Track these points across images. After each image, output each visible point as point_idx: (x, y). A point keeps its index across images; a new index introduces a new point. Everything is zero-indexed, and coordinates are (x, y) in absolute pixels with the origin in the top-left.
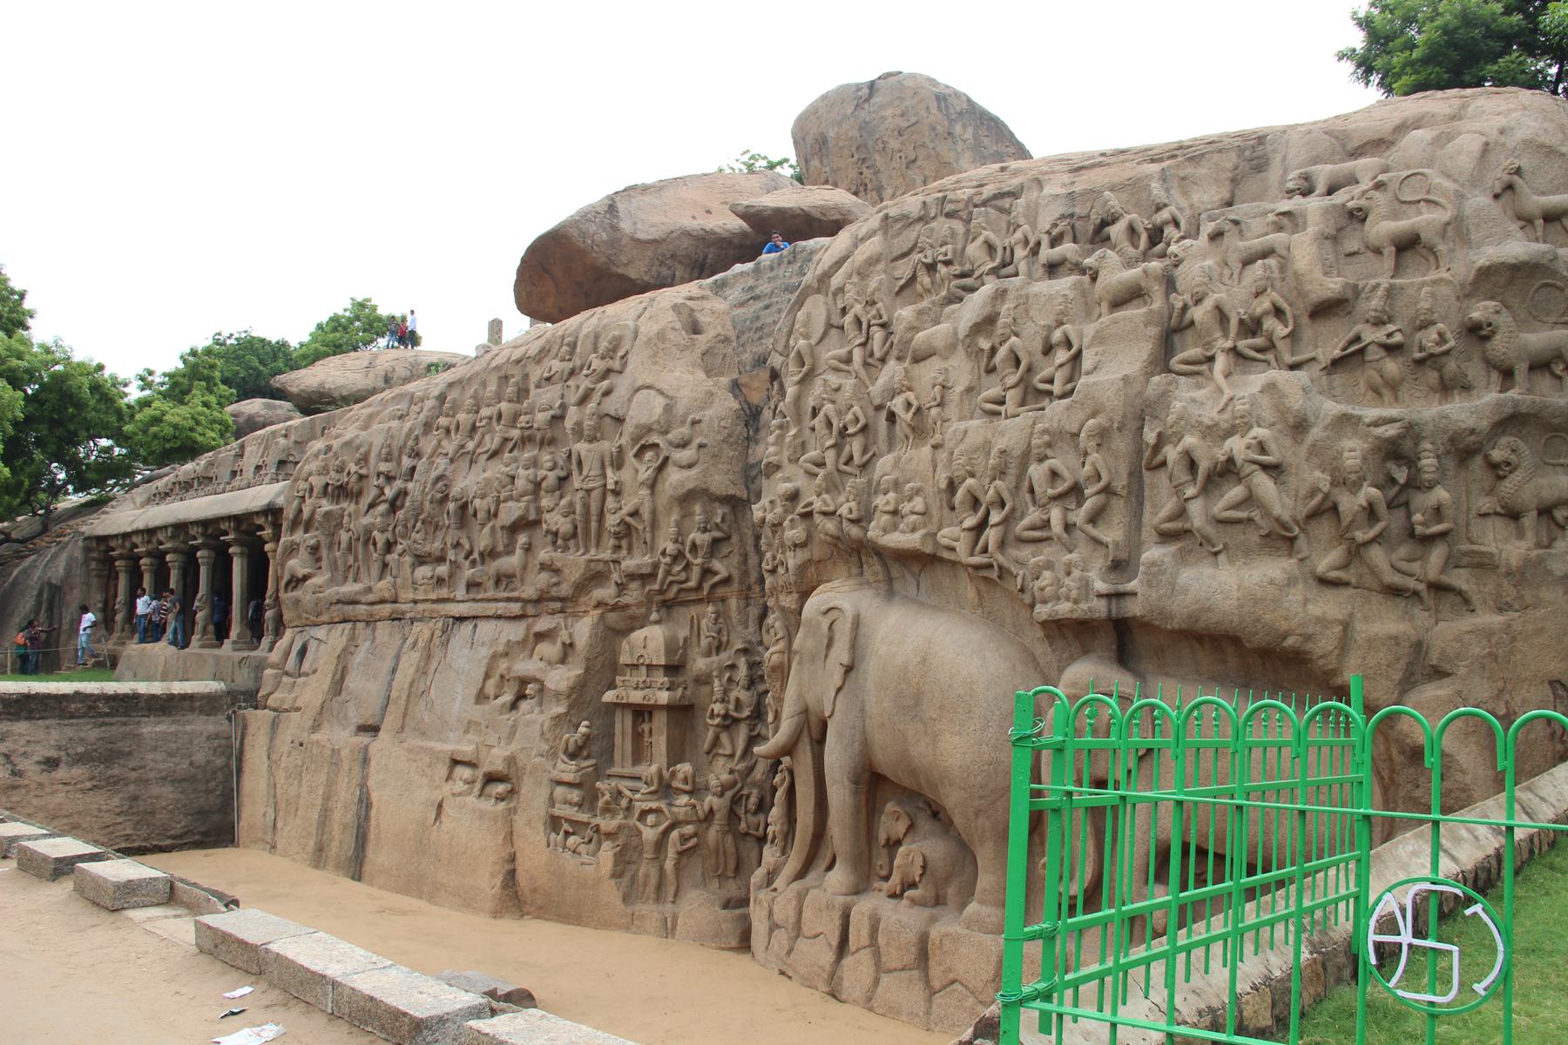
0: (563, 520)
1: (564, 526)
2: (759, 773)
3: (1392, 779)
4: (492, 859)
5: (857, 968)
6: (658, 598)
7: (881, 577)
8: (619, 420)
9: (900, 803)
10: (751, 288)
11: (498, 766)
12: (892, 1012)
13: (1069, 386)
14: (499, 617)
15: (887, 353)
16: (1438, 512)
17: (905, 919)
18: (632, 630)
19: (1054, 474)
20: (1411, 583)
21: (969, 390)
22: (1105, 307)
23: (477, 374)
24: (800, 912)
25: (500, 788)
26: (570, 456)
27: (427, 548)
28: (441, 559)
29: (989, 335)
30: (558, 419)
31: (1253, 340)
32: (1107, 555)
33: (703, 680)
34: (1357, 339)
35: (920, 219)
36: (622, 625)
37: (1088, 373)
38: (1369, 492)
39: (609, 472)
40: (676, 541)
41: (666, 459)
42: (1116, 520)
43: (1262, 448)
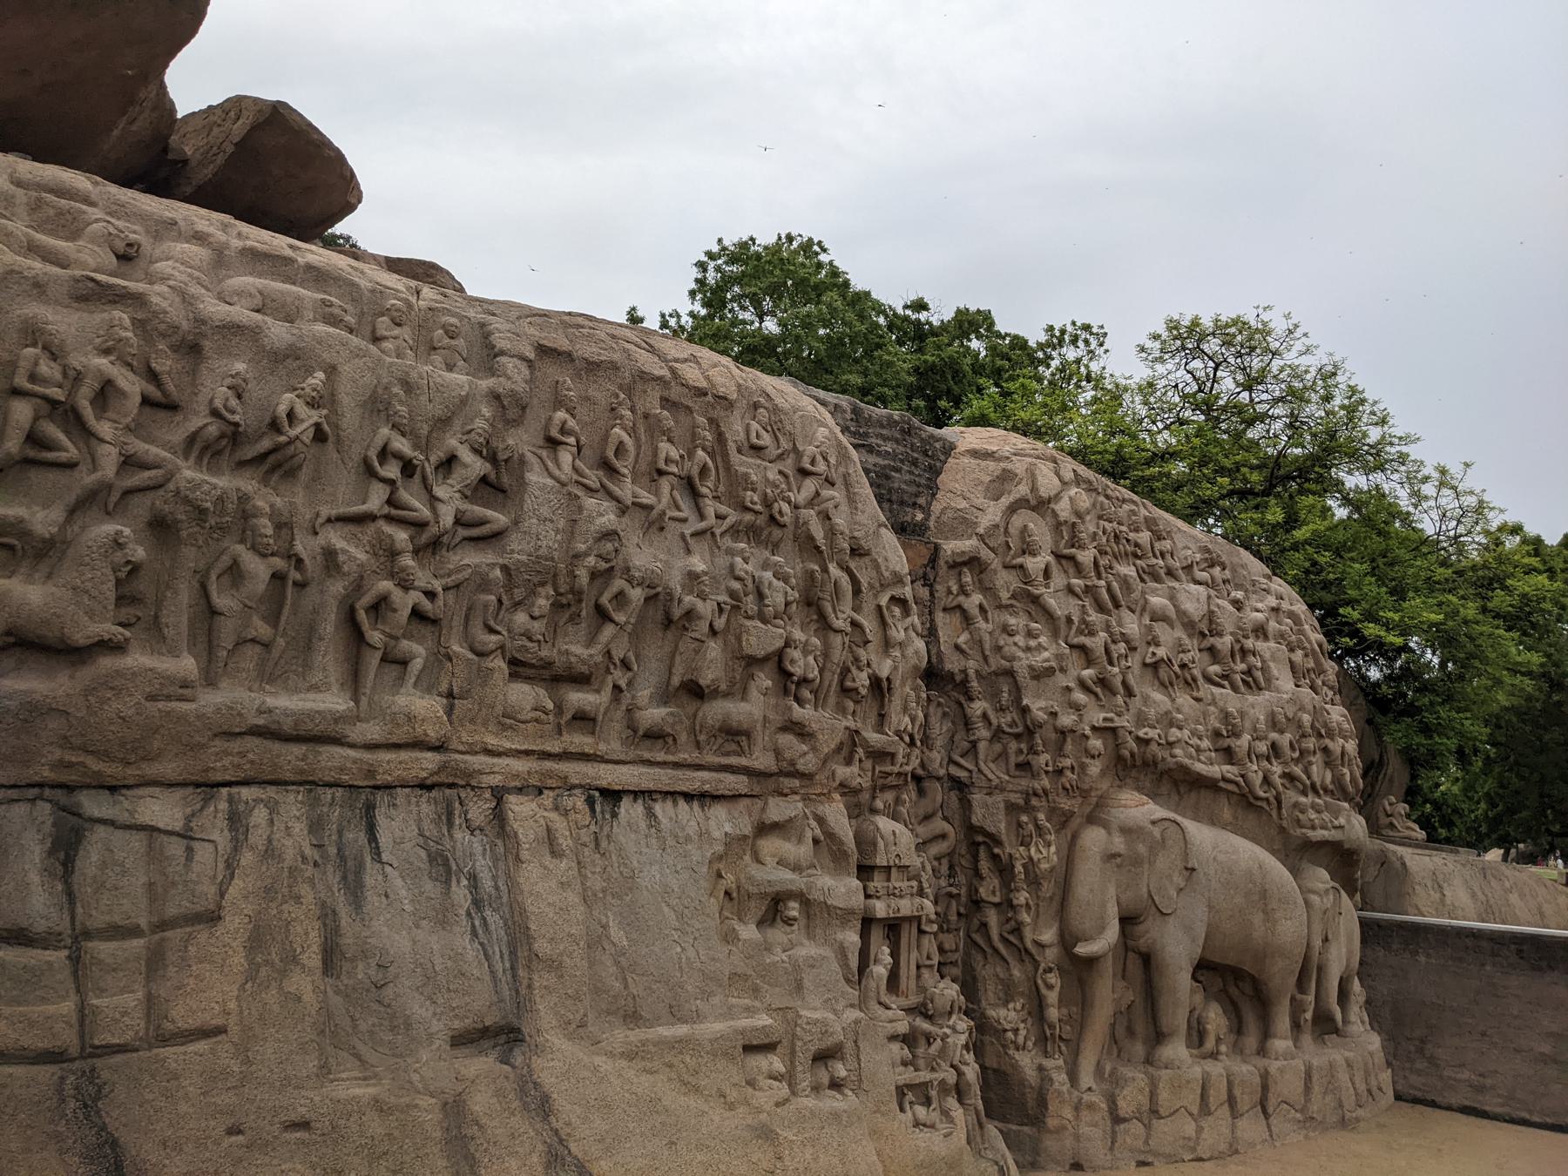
1: (814, 673)
6: (881, 781)
14: (688, 797)
23: (614, 367)
24: (1153, 1095)
25: (840, 1070)
27: (544, 653)
28: (581, 680)
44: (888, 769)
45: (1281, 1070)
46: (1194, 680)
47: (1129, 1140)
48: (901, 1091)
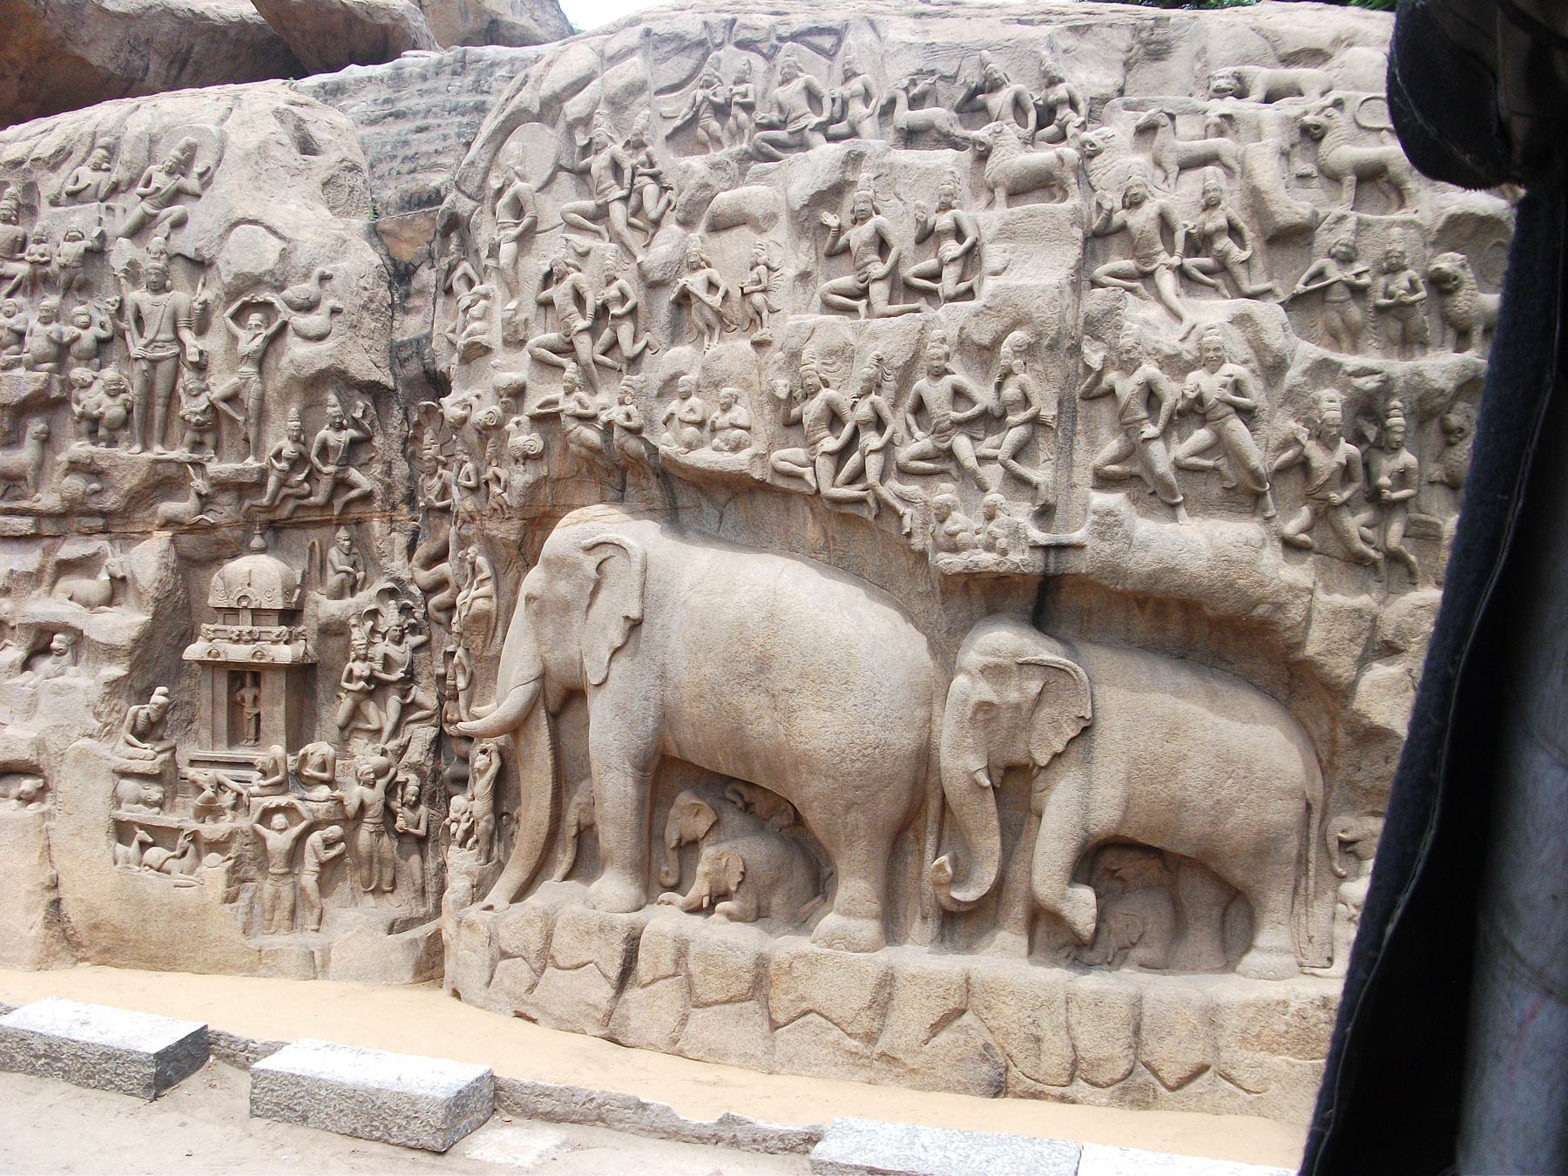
0: (108, 401)
1: (113, 409)
2: (415, 754)
3: (1330, 762)
4: (28, 886)
5: (651, 1006)
6: (263, 517)
7: (658, 505)
8: (200, 265)
9: (698, 794)
10: (387, 101)
11: (24, 753)
12: (713, 1055)
13: (963, 286)
15: (663, 214)
16: (1402, 478)
17: (731, 939)
18: (216, 560)
19: (959, 394)
20: (1372, 553)
21: (804, 276)
22: (1000, 194)
26: (120, 311)
29: (834, 209)
30: (96, 253)
31: (1206, 261)
32: (1033, 500)
33: (335, 631)
34: (1320, 274)
35: (701, 43)
36: (203, 553)
37: (996, 274)
38: (1346, 450)
39: (187, 336)
40: (296, 440)
41: (285, 325)
42: (1042, 456)
43: (1238, 387)
44: (257, 502)
45: (812, 961)
46: (759, 313)
47: (507, 982)
48: (122, 831)
